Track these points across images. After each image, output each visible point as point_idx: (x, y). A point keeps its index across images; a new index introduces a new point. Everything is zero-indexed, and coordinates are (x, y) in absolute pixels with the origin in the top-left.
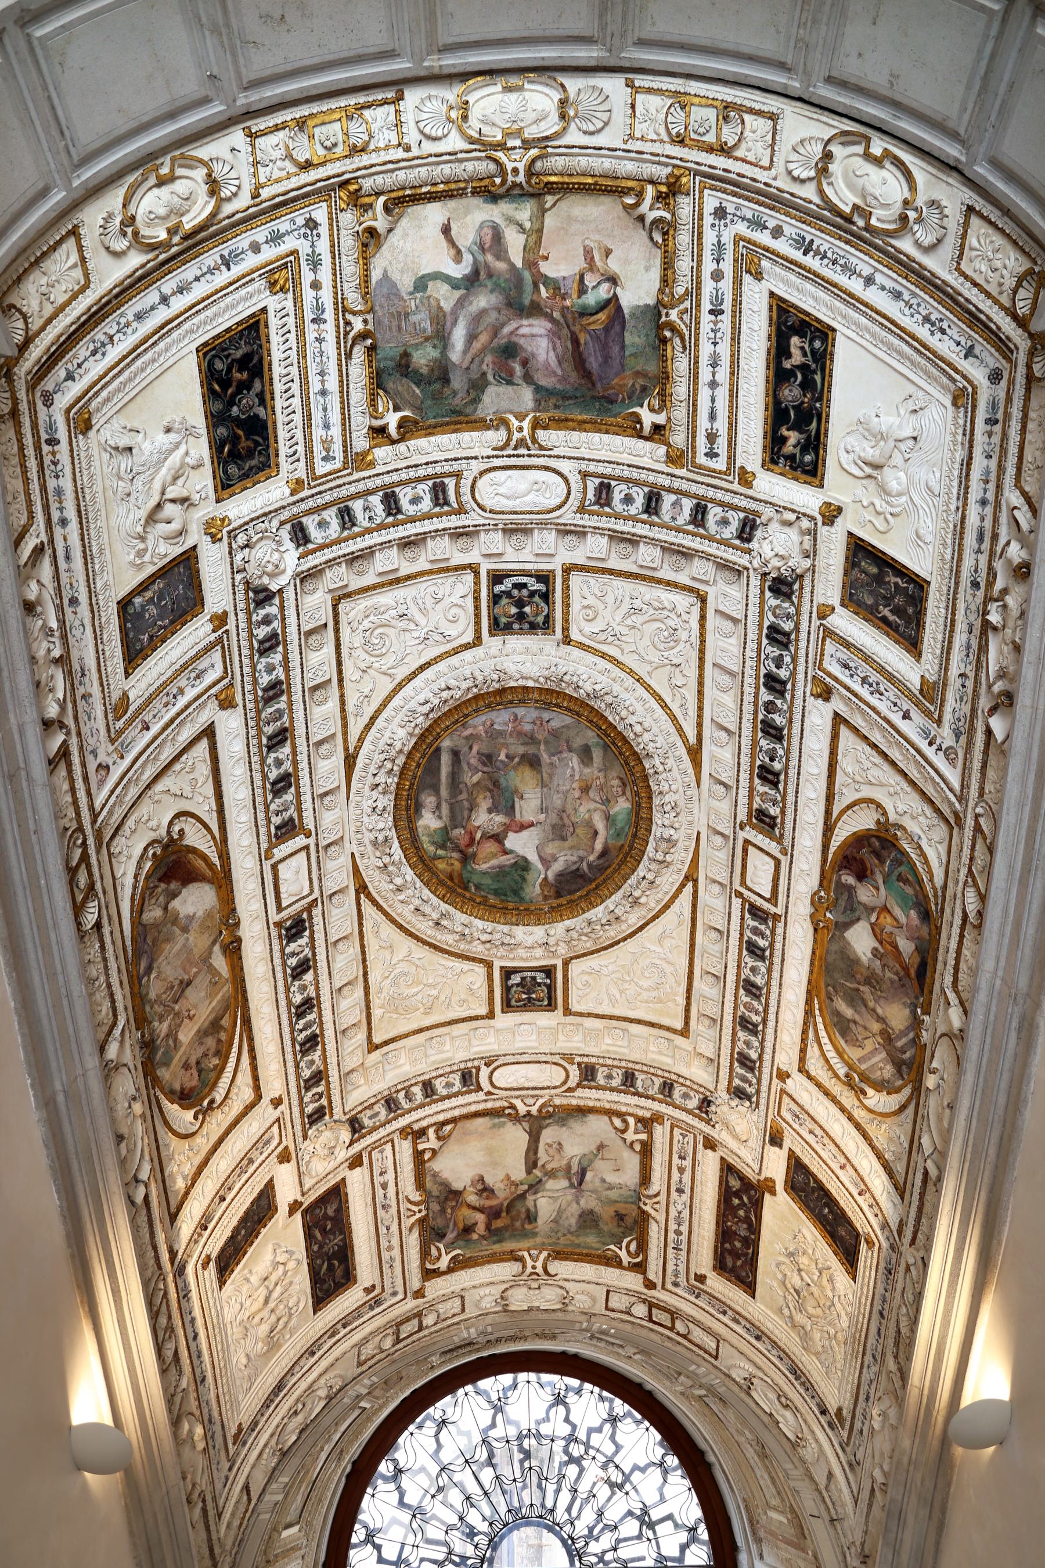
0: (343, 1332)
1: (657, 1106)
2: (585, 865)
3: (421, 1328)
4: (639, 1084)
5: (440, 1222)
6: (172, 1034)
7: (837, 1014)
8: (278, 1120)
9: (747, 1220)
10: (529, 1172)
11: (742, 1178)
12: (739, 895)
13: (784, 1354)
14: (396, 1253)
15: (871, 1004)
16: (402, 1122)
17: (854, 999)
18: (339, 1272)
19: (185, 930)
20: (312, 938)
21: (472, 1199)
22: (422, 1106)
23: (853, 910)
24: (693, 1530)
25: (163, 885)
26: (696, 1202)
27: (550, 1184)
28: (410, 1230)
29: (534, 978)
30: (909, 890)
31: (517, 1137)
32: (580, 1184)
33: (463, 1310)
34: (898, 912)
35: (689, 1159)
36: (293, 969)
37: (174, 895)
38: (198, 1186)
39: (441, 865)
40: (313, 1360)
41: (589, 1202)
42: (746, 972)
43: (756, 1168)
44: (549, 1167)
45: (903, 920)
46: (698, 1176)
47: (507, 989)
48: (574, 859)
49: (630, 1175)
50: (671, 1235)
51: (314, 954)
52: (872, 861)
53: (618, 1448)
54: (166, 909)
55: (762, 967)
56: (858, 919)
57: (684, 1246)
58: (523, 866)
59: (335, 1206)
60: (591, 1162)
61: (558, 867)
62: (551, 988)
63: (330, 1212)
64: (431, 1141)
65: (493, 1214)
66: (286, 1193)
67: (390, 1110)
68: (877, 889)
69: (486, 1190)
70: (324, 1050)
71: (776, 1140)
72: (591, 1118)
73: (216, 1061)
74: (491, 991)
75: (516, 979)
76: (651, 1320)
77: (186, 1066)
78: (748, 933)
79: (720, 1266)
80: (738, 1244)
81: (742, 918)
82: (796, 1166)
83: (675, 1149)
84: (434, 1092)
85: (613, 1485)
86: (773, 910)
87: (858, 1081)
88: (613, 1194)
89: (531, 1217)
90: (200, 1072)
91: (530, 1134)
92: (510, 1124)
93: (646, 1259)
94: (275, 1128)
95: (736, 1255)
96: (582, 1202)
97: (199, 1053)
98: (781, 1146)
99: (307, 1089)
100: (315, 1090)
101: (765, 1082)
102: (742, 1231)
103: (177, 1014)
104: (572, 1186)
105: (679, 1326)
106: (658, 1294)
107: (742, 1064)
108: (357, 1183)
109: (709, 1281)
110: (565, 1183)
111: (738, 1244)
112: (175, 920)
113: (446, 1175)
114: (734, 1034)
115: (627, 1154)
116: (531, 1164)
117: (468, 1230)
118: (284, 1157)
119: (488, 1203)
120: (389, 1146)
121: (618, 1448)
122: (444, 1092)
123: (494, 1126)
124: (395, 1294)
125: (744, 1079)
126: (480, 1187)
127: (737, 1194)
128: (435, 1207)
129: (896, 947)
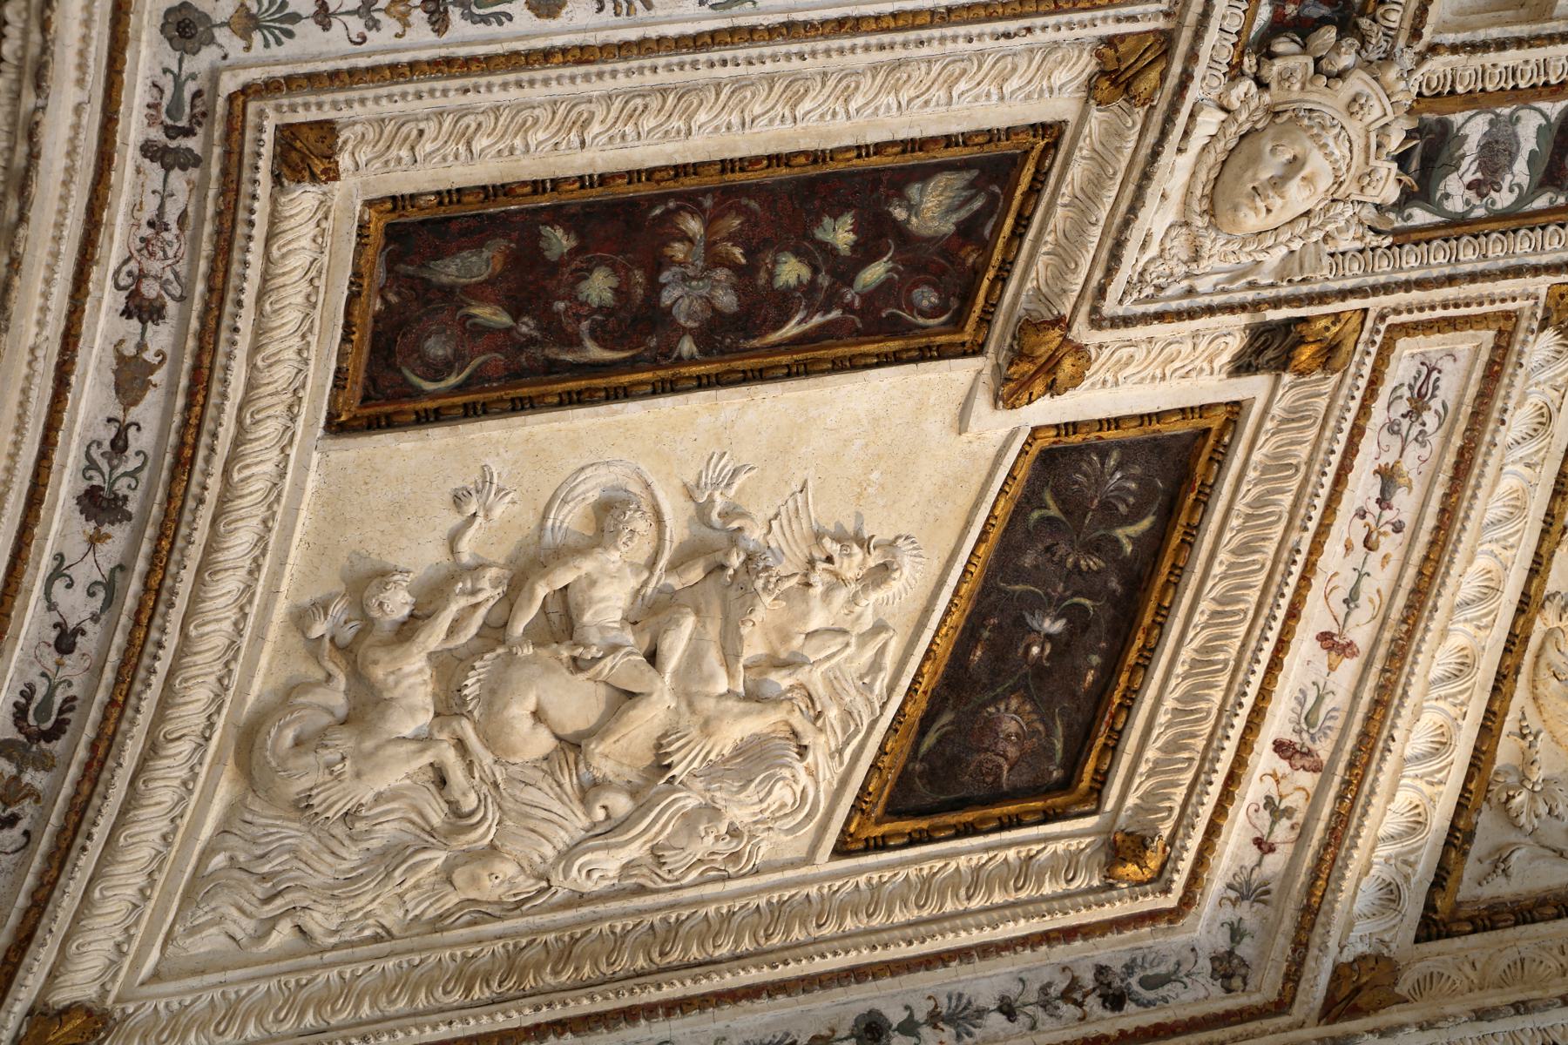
71: (1271, 348)
101: (1523, 248)
109: (304, 199)
111: (599, 287)
125: (1495, 156)
127: (879, 234)
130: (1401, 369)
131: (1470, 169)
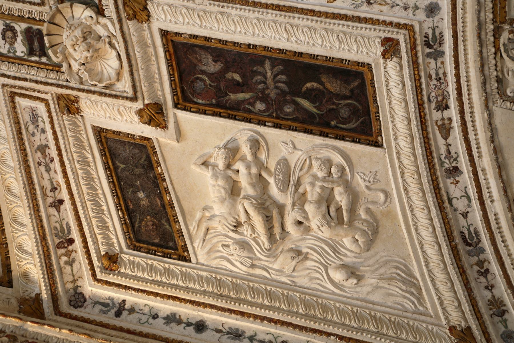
8: (12, 95)
18: (333, 86)
59: (208, 59)
63: (212, 67)
94: (23, 103)
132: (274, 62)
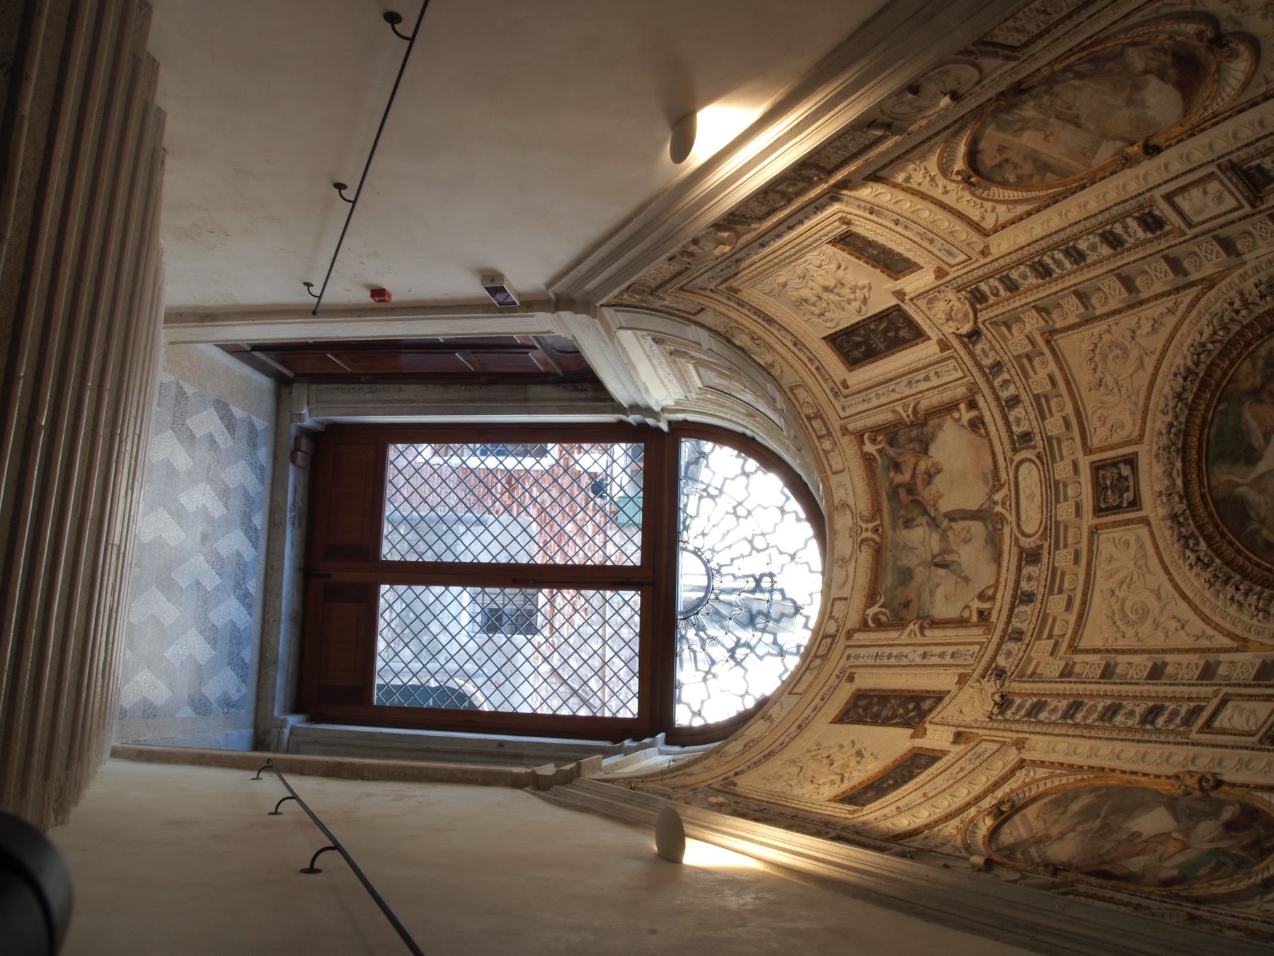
0: (813, 368)
1: (1000, 626)
2: (1255, 526)
3: (819, 437)
4: (1023, 608)
5: (902, 439)
6: (1026, 124)
7: (1076, 796)
8: (970, 258)
9: (895, 716)
10: (946, 515)
11: (930, 710)
12: (1216, 694)
13: (784, 746)
14: (875, 402)
15: (1080, 828)
16: (981, 382)
17: (1088, 813)
18: (856, 354)
19: (1130, 102)
20: (1144, 243)
21: (922, 465)
22: (997, 398)
23: (1190, 816)
24: (699, 713)
25: (1169, 60)
26: (913, 671)
27: (936, 536)
28: (893, 411)
29: (1127, 489)
30: (1202, 872)
31: (973, 498)
32: (937, 565)
33: (834, 473)
34: (1180, 859)
35: (952, 661)
36: (1111, 232)
37: (1162, 76)
38: (901, 195)
39: (1246, 368)
40: (790, 345)
41: (920, 574)
42: (1128, 705)
43: (936, 720)
44: (950, 534)
45: (1168, 864)
46: (935, 670)
47: (1114, 463)
48: (1263, 512)
49: (941, 610)
50: (888, 650)
51: (1129, 250)
52: (1246, 837)
53: (761, 658)
54: (1146, 72)
55: (1134, 722)
56: (1177, 820)
57: (879, 662)
58: (1251, 456)
59: (907, 336)
60: (954, 572)
61: (1253, 496)
62: (1117, 509)
63: (903, 333)
64: (966, 415)
65: (910, 488)
66: (913, 284)
67: (991, 367)
68: (1212, 841)
69: (929, 477)
70: (1037, 287)
71: (958, 738)
72: (994, 567)
73: (1012, 179)
74: (1112, 448)
75: (1125, 471)
76: (823, 637)
77: (1001, 149)
78: (1171, 706)
79: (860, 695)
80: (875, 709)
81: (1190, 699)
82: (931, 757)
83: (961, 648)
84: (1011, 407)
85: (732, 652)
86: (1195, 728)
87: (1003, 814)
88: (926, 596)
89: (908, 524)
90: (999, 165)
91: (979, 511)
92: (987, 490)
93: (871, 630)
94: (962, 257)
95: (866, 709)
96: (920, 568)
97: (1017, 159)
98: (954, 743)
99: (1001, 280)
100: (1001, 288)
102: (886, 713)
103: (1045, 122)
104: (934, 557)
105: (818, 661)
106: (841, 642)
107: (1034, 706)
108: (926, 351)
110: (936, 551)
111: (875, 709)
112: (1137, 87)
113: (941, 437)
114: (1065, 696)
115: (961, 605)
116: (952, 517)
117: (897, 467)
118: (940, 273)
119: (919, 481)
120: (960, 374)
121: (761, 658)
122: (1011, 418)
123: (985, 475)
124: (844, 409)
125: (1020, 708)
126: (932, 471)
127: (917, 707)
128: (914, 433)
129: (1138, 854)
130: (979, 749)
131: (1013, 710)
132: (881, 352)
